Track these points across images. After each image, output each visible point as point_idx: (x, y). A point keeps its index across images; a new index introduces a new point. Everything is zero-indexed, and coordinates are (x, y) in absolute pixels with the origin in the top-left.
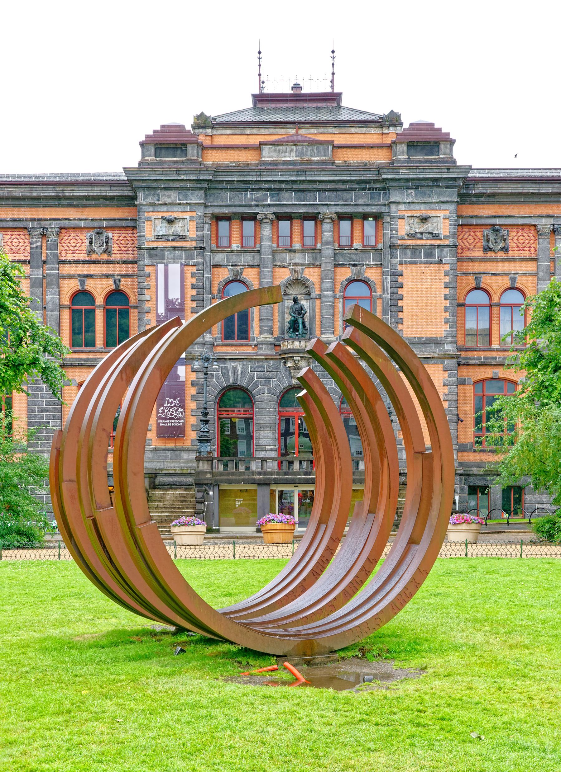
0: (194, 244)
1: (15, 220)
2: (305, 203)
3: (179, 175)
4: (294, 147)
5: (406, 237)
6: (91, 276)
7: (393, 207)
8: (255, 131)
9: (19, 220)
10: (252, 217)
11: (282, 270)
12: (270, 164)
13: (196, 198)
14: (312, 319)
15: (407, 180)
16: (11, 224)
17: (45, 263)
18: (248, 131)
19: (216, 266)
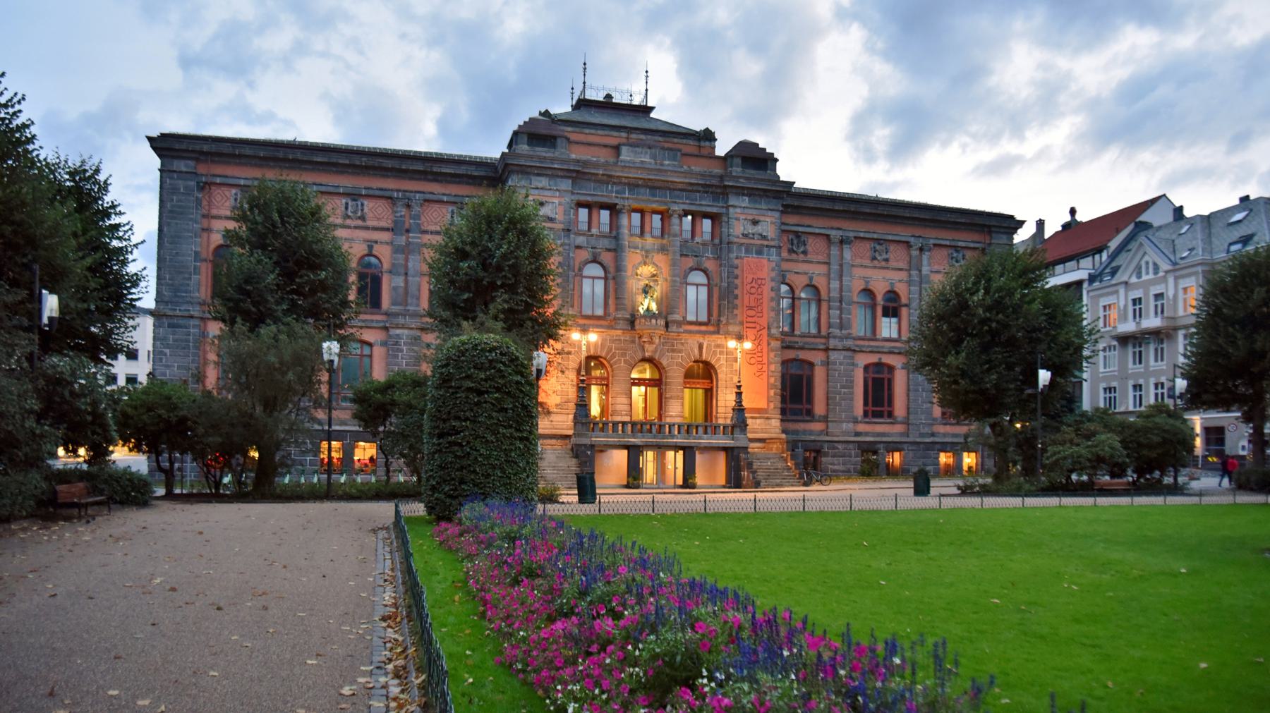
0: (561, 226)
1: (381, 189)
2: (657, 199)
3: (553, 163)
4: (649, 150)
5: (741, 236)
7: (731, 210)
8: (593, 131)
9: (386, 190)
10: (612, 208)
11: (634, 255)
12: (629, 162)
13: (566, 185)
15: (743, 188)
16: (377, 193)
17: (408, 231)
18: (587, 131)
19: (578, 247)
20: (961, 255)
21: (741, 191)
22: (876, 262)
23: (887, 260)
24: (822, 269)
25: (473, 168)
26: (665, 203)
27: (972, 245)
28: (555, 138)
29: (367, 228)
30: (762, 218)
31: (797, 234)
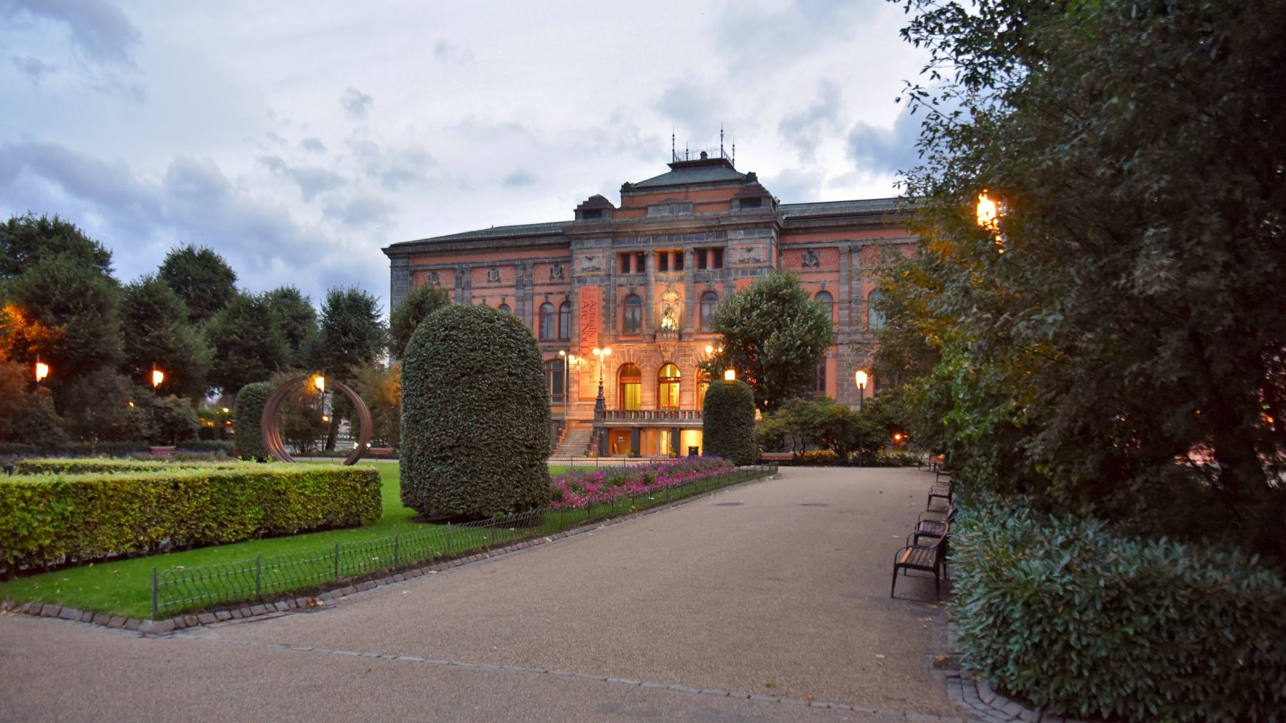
6: (551, 293)
19: (621, 285)
21: (736, 227)
24: (834, 276)
25: (559, 238)
26: (680, 245)
29: (501, 287)
30: (754, 246)
31: (810, 251)
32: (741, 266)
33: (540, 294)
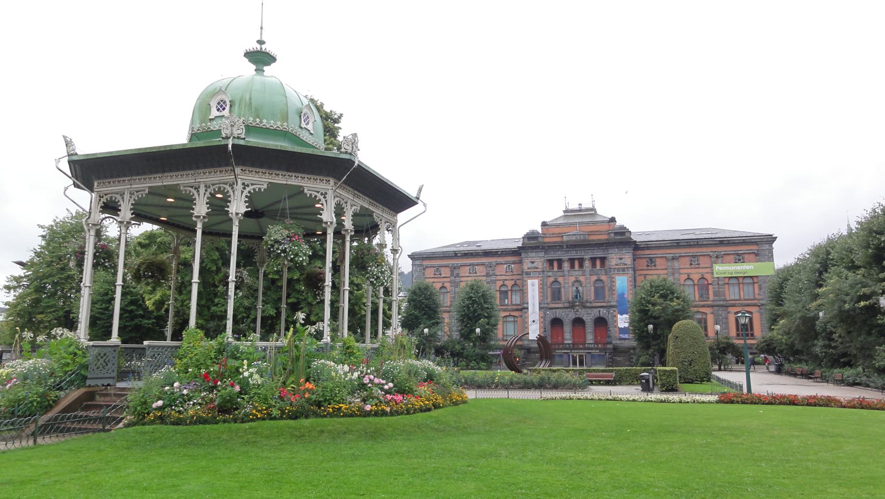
6: (506, 280)
14: (583, 294)
19: (549, 277)
20: (741, 257)
22: (693, 266)
23: (699, 264)
27: (747, 252)
28: (538, 237)
31: (651, 259)
32: (616, 267)
33: (500, 280)
